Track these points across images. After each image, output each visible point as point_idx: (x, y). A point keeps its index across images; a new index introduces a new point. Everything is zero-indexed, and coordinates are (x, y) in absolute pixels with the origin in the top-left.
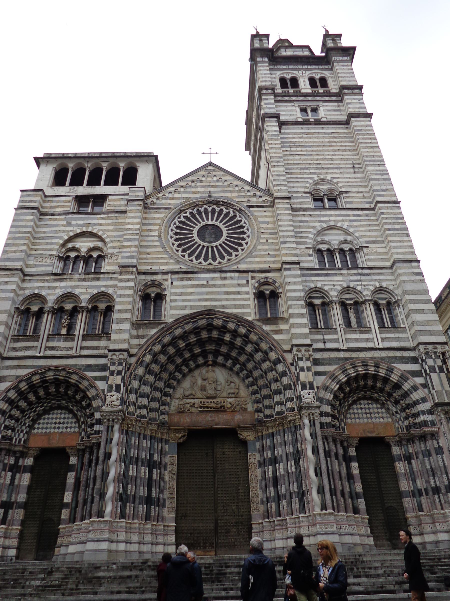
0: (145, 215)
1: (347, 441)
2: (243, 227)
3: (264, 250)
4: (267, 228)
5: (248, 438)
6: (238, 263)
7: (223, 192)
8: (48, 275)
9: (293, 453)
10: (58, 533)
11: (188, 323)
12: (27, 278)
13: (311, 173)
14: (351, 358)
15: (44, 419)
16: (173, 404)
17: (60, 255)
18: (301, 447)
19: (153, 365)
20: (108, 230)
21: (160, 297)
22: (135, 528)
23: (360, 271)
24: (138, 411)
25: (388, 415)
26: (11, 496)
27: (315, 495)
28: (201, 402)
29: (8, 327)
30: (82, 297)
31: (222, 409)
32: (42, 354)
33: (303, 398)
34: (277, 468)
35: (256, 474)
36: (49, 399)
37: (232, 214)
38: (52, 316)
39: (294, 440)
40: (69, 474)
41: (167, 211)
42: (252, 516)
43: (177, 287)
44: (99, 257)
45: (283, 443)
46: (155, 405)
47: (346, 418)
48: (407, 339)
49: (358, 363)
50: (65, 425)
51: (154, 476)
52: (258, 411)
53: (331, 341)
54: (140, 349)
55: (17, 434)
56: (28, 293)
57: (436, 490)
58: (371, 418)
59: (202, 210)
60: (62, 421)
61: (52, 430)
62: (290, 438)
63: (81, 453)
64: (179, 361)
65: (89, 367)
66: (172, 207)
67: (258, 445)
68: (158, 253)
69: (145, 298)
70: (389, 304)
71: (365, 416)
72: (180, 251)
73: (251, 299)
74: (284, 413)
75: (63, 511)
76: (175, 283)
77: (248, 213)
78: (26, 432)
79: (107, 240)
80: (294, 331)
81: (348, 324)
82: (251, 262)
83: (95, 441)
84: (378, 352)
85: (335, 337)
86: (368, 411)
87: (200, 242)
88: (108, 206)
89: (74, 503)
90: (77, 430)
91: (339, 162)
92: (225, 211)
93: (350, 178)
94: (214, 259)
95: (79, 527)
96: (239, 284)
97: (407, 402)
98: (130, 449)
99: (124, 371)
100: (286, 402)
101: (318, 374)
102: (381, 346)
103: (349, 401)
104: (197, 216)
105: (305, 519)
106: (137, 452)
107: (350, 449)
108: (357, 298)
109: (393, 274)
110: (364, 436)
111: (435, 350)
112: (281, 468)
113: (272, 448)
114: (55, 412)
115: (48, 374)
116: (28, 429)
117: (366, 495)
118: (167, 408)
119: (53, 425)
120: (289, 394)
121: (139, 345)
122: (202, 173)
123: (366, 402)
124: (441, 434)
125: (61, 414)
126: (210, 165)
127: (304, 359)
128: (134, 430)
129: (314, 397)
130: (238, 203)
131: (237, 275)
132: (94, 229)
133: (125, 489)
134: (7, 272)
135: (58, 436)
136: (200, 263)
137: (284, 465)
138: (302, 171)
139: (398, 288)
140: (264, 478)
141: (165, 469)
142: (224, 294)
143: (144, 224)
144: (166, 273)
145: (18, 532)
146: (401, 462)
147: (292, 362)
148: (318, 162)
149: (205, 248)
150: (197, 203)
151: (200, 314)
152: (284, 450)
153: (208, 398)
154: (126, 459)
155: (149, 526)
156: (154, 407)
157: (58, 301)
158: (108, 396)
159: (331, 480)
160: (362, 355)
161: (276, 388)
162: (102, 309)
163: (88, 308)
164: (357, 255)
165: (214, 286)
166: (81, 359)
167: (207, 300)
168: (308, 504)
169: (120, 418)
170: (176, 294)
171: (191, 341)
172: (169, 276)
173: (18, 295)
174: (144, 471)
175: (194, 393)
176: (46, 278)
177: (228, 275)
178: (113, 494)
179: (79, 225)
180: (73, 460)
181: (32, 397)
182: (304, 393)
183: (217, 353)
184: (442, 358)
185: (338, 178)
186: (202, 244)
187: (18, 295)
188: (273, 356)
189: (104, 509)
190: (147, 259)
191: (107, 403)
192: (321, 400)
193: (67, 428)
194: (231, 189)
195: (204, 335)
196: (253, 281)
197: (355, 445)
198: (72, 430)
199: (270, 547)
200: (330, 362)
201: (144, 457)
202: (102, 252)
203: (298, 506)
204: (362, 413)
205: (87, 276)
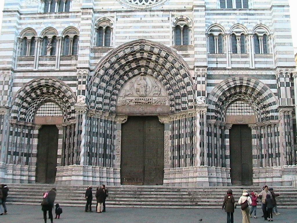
1: (225, 127)
5: (165, 122)
6: (163, 4)
8: (35, 14)
9: (190, 133)
10: (56, 170)
12: (22, 16)
15: (42, 108)
16: (119, 100)
18: (194, 130)
19: (105, 76)
21: (108, 29)
23: (248, 12)
25: (253, 111)
26: (29, 151)
27: (198, 158)
28: (136, 99)
29: (15, 51)
30: (58, 30)
32: (36, 69)
33: (197, 101)
34: (180, 141)
35: (168, 143)
36: (43, 96)
38: (40, 43)
40: (59, 139)
42: (165, 166)
45: (185, 126)
46: (107, 101)
47: (226, 112)
48: (271, 63)
49: (237, 78)
50: (54, 112)
52: (171, 106)
53: (221, 62)
54: (96, 67)
55: (28, 117)
56: (24, 27)
57: (271, 156)
58: (242, 112)
60: (52, 109)
61: (47, 115)
62: (189, 124)
65: (66, 78)
67: (170, 126)
70: (265, 35)
71: (238, 111)
73: (170, 32)
75: (58, 159)
78: (33, 116)
80: (196, 56)
81: (235, 50)
83: (72, 123)
84: (251, 71)
86: (240, 108)
89: (63, 156)
90: (61, 115)
95: (67, 168)
96: (162, 21)
97: (265, 104)
98: (93, 128)
99: (87, 82)
100: (188, 102)
101: (209, 85)
102: (253, 68)
105: (192, 169)
106: (97, 129)
107: (226, 130)
109: (271, 14)
110: (235, 123)
111: (287, 72)
112: (182, 141)
114: (48, 103)
115: (42, 81)
116: (33, 114)
118: (114, 103)
119: (47, 112)
120: (190, 97)
121: (96, 64)
123: (240, 102)
124: (280, 124)
125: (51, 105)
127: (201, 76)
128: (95, 117)
129: (204, 101)
131: (162, 13)
133: (91, 149)
134: (9, 13)
136: (137, 3)
137: (184, 139)
139: (272, 26)
142: (152, 28)
144: (114, 12)
145: (35, 169)
146: (255, 139)
147: (194, 76)
151: (136, 43)
152: (185, 131)
153: (140, 96)
154: (90, 133)
156: (107, 102)
157: (43, 33)
158: (78, 98)
159: (210, 149)
160: (240, 72)
162: (71, 40)
163: (62, 38)
165: (146, 21)
166: (60, 73)
167: (140, 32)
169: (86, 110)
170: (120, 28)
171: (130, 60)
173: (18, 29)
175: (132, 94)
176: (34, 16)
177: (156, 13)
178: (84, 152)
180: (61, 132)
181: (33, 95)
182: (198, 98)
183: (147, 67)
184: (290, 77)
187: (18, 29)
188: (182, 72)
189: (80, 160)
191: (78, 101)
192: (210, 102)
193: (55, 113)
195: (138, 56)
196: (173, 18)
197: (229, 128)
200: (219, 77)
201: (101, 132)
203: (189, 162)
205: (61, 15)
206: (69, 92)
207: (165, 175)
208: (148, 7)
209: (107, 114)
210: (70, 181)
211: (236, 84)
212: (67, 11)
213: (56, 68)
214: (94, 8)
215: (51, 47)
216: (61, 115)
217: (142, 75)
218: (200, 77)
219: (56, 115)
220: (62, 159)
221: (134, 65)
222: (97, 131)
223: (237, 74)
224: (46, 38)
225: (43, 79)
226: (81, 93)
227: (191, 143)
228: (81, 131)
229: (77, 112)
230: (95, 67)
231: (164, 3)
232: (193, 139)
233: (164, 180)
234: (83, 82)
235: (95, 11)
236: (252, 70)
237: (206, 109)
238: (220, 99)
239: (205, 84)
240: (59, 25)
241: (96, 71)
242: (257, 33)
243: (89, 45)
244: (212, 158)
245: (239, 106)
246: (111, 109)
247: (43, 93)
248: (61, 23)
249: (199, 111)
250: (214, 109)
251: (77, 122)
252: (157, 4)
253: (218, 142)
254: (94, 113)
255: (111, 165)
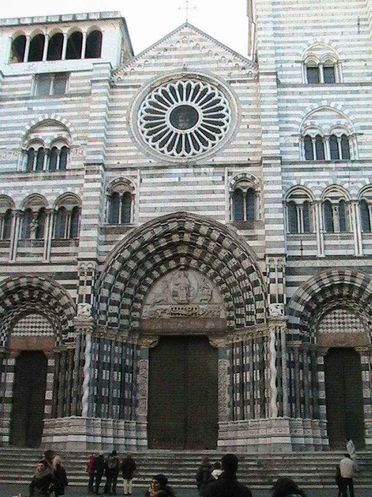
0: (111, 97)
2: (222, 108)
3: (244, 139)
4: (248, 110)
5: (219, 345)
6: (214, 155)
7: (200, 63)
8: (12, 173)
10: (44, 426)
11: (158, 226)
13: (307, 35)
14: (327, 268)
15: (21, 322)
16: (144, 310)
17: (24, 148)
18: (267, 358)
20: (72, 118)
21: (128, 197)
22: (110, 425)
23: (350, 165)
24: (109, 319)
25: (362, 325)
27: (273, 405)
30: (48, 198)
31: (194, 316)
32: (13, 261)
33: (270, 312)
34: (244, 376)
35: (224, 380)
37: (210, 92)
39: (261, 351)
40: (49, 375)
41: (136, 90)
43: (147, 185)
44: (64, 148)
45: (251, 352)
46: (126, 312)
47: (318, 328)
49: (335, 272)
50: (41, 329)
51: (127, 379)
52: (230, 319)
53: (309, 248)
54: (109, 256)
58: (344, 328)
59: (176, 86)
61: (29, 334)
62: (258, 349)
63: (58, 356)
64: (149, 265)
65: (60, 276)
66: (141, 84)
67: (228, 351)
68: (126, 144)
69: (113, 197)
71: (338, 325)
72: (150, 140)
74: (253, 324)
75: (46, 406)
76: (144, 180)
77: (228, 90)
79: (71, 130)
80: (268, 238)
81: (330, 228)
82: (229, 155)
83: (69, 347)
85: (313, 243)
86: (341, 321)
87: (172, 128)
88: (71, 86)
90: (52, 334)
91: (342, 17)
92: (202, 88)
93: (352, 40)
94: (188, 150)
95: (61, 422)
96: (213, 181)
99: (93, 281)
101: (289, 284)
102: (361, 254)
103: (322, 311)
104: (170, 95)
106: (109, 358)
108: (344, 197)
112: (248, 376)
113: (241, 357)
114: (31, 316)
117: (327, 402)
118: (138, 314)
119: (30, 329)
120: (260, 305)
121: (108, 252)
122: (176, 37)
123: (341, 311)
125: (36, 318)
126: (186, 26)
127: (276, 270)
128: (106, 338)
129: (282, 310)
130: (217, 77)
131: (212, 170)
132: (56, 116)
133: (99, 391)
135: (35, 339)
136: (173, 155)
138: (295, 31)
140: (232, 384)
141: (137, 372)
143: (110, 108)
145: (8, 422)
146: (367, 372)
147: (265, 271)
148: (316, 18)
149: (178, 136)
150: (170, 79)
151: (171, 217)
152: (251, 360)
154: (98, 365)
155: (122, 423)
157: (25, 203)
158: (79, 307)
159: (293, 389)
160: (340, 263)
161: (248, 297)
162: (68, 214)
163: (55, 210)
164: (351, 143)
165: (187, 183)
166: (51, 266)
167: (178, 201)
168: (268, 410)
169: (91, 328)
170: (145, 194)
171: (162, 246)
172: (136, 173)
174: (116, 375)
175: (165, 299)
177: (203, 170)
178: (89, 396)
179: (41, 112)
180: (51, 363)
182: (272, 306)
183: (189, 256)
185: (337, 41)
186: (175, 130)
188: (246, 263)
190: (114, 152)
191: (78, 313)
192: (290, 312)
193: (43, 332)
194: (209, 58)
195: (176, 238)
196: (230, 177)
198: (48, 334)
199: (233, 444)
201: (116, 362)
202: (66, 143)
203: (259, 411)
204: (335, 323)
205: (53, 174)
206: (65, 297)
207: (219, 433)
208: (189, 160)
209: (126, 334)
210: (66, 442)
211: (332, 283)
212: (63, 167)
213: (44, 259)
214: (106, 163)
215: (36, 225)
216: (52, 334)
217: (182, 270)
218: (274, 271)
219: (45, 334)
220: (52, 407)
221: (168, 254)
222: (109, 361)
223: (334, 265)
224: (29, 210)
225: (24, 277)
226: (84, 300)
227: (262, 379)
228: (84, 362)
229: (78, 330)
230: (105, 257)
231: (217, 154)
232: (265, 373)
233: (218, 441)
234: (87, 281)
235: (106, 167)
236: (359, 258)
237: (285, 324)
238: (307, 307)
239: (282, 283)
240: (49, 191)
241: (107, 263)
242: (365, 198)
243: (97, 223)
244: (298, 403)
245: (339, 318)
246: (132, 324)
247: (23, 300)
248: (54, 188)
249: (274, 327)
250: (298, 322)
251: (77, 347)
252: (205, 156)
253: (305, 378)
254: (105, 332)
255: (133, 416)
